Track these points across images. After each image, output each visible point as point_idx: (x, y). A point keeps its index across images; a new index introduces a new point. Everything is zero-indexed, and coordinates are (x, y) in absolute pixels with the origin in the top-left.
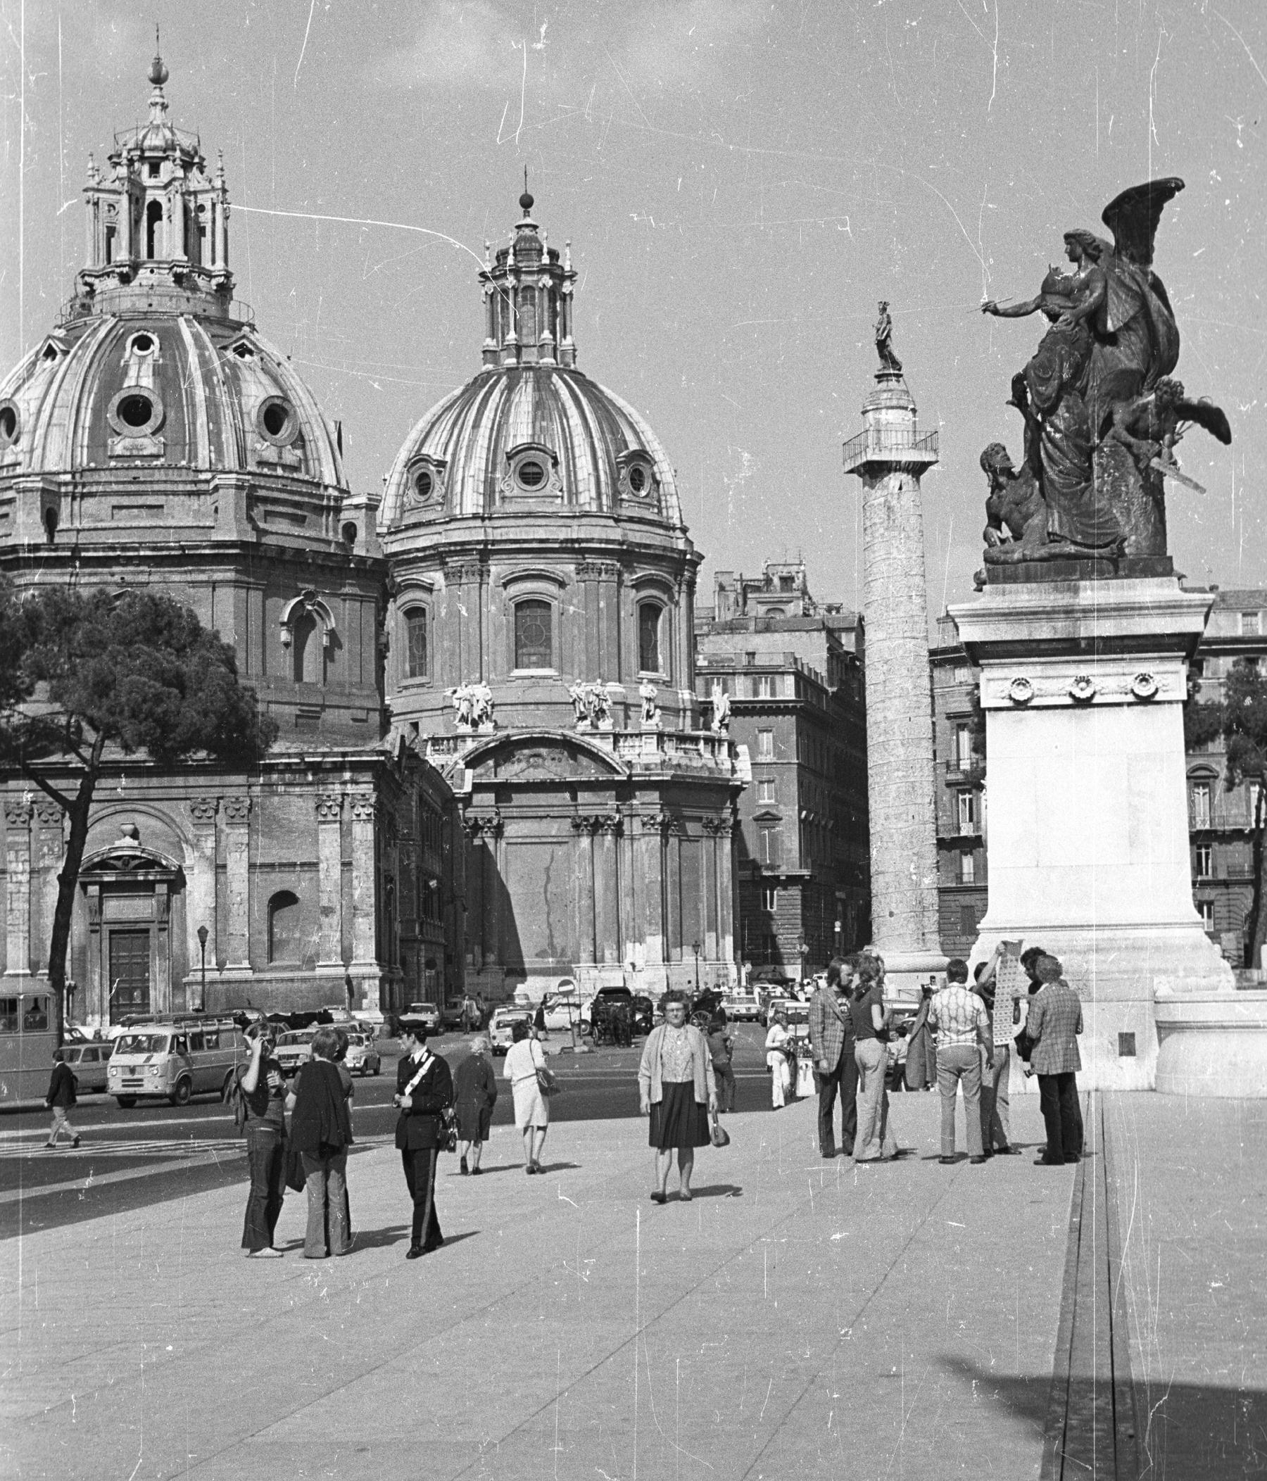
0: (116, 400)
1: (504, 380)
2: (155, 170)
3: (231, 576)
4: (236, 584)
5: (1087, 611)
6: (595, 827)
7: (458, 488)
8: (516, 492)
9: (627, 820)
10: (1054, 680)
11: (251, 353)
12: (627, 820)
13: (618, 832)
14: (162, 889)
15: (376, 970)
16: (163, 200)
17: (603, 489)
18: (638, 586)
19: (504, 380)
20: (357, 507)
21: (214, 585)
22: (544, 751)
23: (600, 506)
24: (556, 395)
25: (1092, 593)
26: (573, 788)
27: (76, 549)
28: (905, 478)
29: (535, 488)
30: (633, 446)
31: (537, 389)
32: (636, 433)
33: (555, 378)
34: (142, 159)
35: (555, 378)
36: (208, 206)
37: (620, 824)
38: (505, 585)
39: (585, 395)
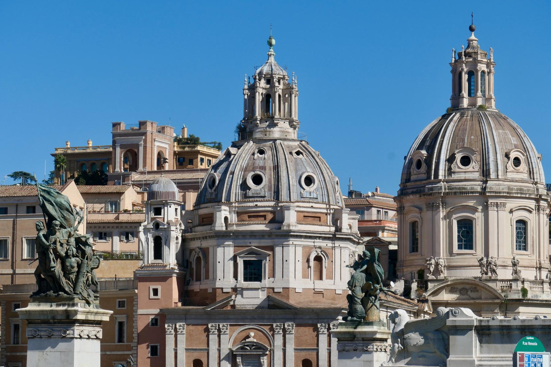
1: (458, 115)
8: (457, 170)
19: (458, 115)
29: (467, 167)
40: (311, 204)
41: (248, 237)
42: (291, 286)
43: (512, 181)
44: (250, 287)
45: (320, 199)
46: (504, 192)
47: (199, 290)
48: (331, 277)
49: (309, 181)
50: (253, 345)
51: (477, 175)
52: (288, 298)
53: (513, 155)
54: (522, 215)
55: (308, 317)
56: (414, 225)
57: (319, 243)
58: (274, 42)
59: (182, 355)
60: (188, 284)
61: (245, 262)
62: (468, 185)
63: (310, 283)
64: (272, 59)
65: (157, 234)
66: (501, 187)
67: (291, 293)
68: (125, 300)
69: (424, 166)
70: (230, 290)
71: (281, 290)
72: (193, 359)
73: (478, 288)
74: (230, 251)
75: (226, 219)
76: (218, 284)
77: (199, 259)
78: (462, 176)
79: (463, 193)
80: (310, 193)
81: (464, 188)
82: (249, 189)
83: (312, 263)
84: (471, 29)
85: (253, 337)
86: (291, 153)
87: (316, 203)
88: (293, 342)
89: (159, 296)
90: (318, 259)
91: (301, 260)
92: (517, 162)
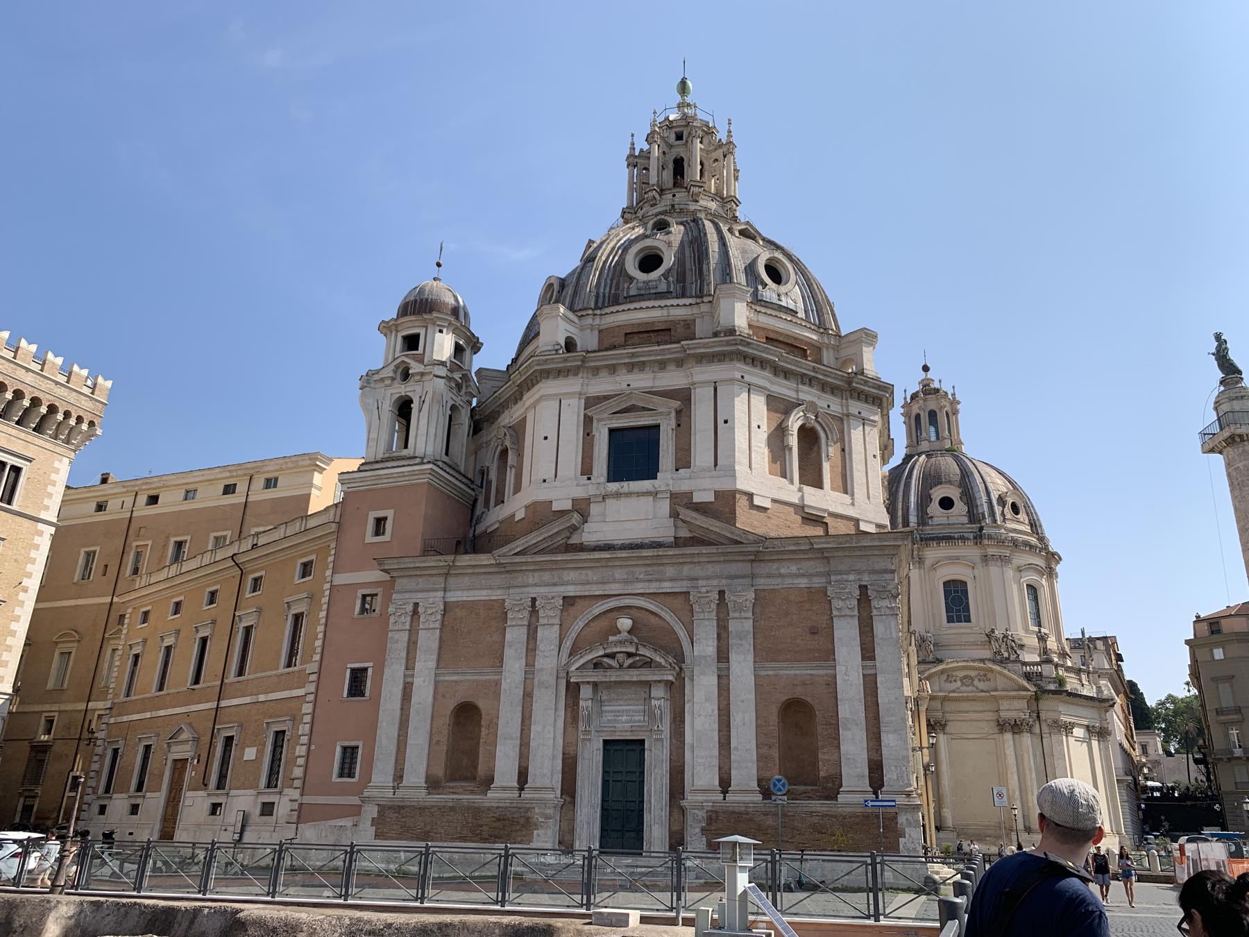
6: (1016, 727)
14: (658, 692)
22: (973, 673)
41: (624, 371)
42: (741, 485)
43: (1015, 531)
44: (626, 490)
45: (801, 314)
47: (497, 526)
48: (845, 486)
50: (630, 655)
51: (965, 520)
52: (731, 518)
53: (1010, 501)
54: (1031, 577)
55: (793, 569)
57: (808, 394)
58: (689, 83)
59: (423, 693)
60: (479, 521)
61: (611, 431)
62: (955, 532)
63: (790, 491)
65: (401, 389)
67: (742, 503)
68: (313, 557)
70: (568, 505)
71: (709, 497)
72: (451, 704)
73: (990, 675)
75: (570, 345)
76: (542, 495)
77: (504, 453)
82: (631, 279)
83: (793, 441)
86: (730, 230)
88: (748, 644)
89: (386, 537)
90: (808, 436)
91: (764, 427)
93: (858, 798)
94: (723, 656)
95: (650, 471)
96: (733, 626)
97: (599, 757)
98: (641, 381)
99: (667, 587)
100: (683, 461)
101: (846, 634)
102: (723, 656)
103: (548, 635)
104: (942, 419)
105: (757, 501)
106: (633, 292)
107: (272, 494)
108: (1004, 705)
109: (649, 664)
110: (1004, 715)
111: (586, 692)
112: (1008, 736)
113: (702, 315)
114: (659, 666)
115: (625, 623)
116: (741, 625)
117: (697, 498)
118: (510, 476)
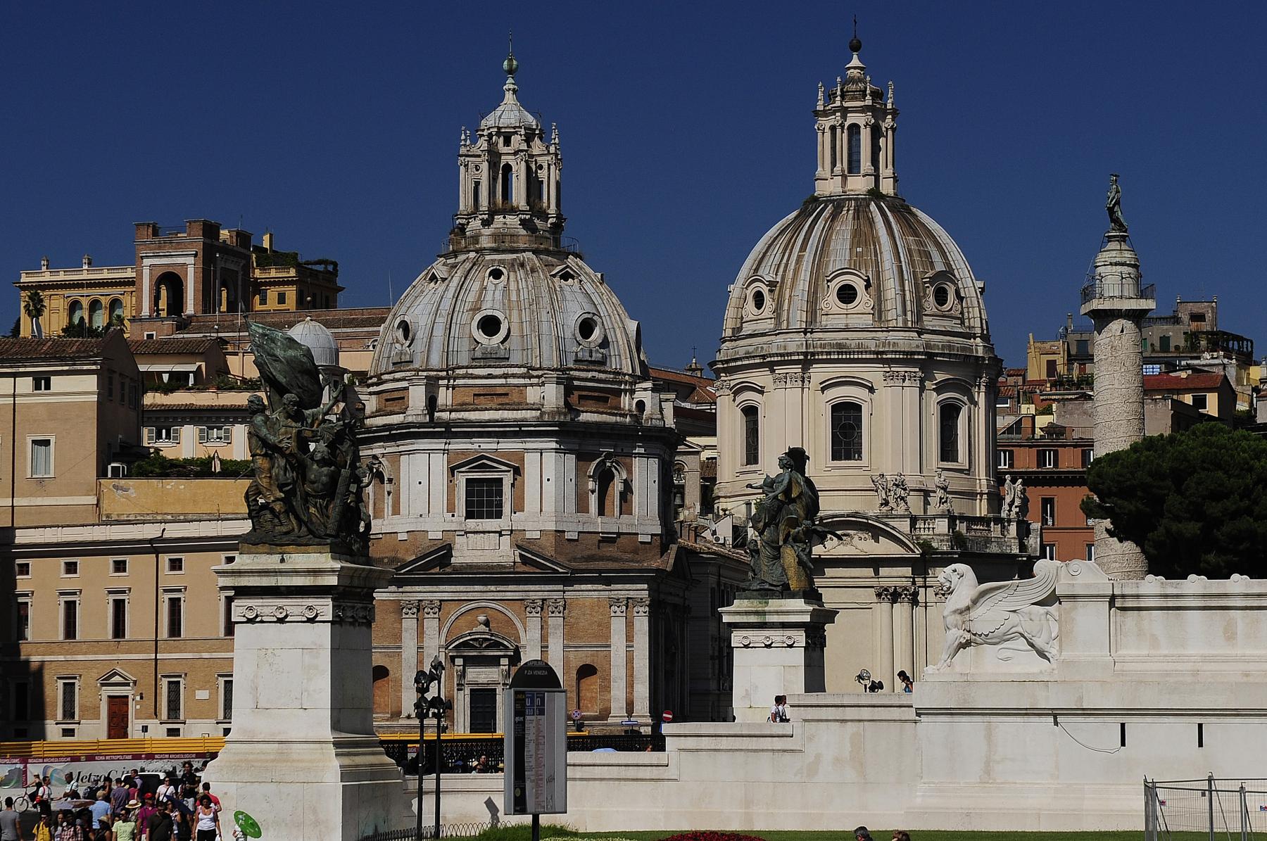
0: (478, 317)
2: (507, 142)
3: (554, 445)
4: (557, 451)
5: (770, 613)
7: (786, 307)
8: (835, 310)
9: (922, 591)
10: (757, 636)
11: (573, 277)
12: (922, 591)
13: (914, 602)
14: (504, 661)
15: (650, 721)
16: (512, 163)
17: (909, 308)
18: (940, 389)
20: (645, 390)
21: (541, 452)
23: (905, 321)
24: (871, 223)
25: (774, 604)
26: (876, 563)
27: (448, 425)
28: (1128, 324)
29: (850, 306)
30: (940, 267)
31: (857, 217)
32: (943, 254)
33: (873, 206)
34: (499, 134)
35: (873, 206)
36: (545, 166)
37: (916, 594)
38: (823, 390)
39: (898, 221)
40: (590, 375)
46: (919, 353)
49: (586, 328)
51: (868, 320)
56: (751, 412)
61: (469, 482)
62: (851, 339)
64: (509, 98)
66: (914, 343)
69: (768, 302)
71: (537, 535)
74: (440, 463)
78: (840, 322)
79: (843, 354)
80: (591, 352)
81: (844, 346)
84: (856, 48)
85: (487, 623)
87: (600, 372)
88: (560, 632)
92: (941, 297)
93: (619, 720)
94: (544, 638)
95: (499, 515)
96: (550, 621)
97: (468, 699)
98: (487, 445)
99: (509, 596)
100: (518, 507)
101: (618, 626)
102: (544, 638)
103: (431, 625)
104: (865, 135)
105: (567, 536)
106: (478, 354)
107: (42, 399)
108: (883, 571)
109: (497, 645)
110: (885, 583)
111: (459, 661)
112: (886, 606)
113: (532, 385)
114: (506, 648)
115: (482, 618)
116: (555, 622)
117: (528, 535)
118: (389, 501)
